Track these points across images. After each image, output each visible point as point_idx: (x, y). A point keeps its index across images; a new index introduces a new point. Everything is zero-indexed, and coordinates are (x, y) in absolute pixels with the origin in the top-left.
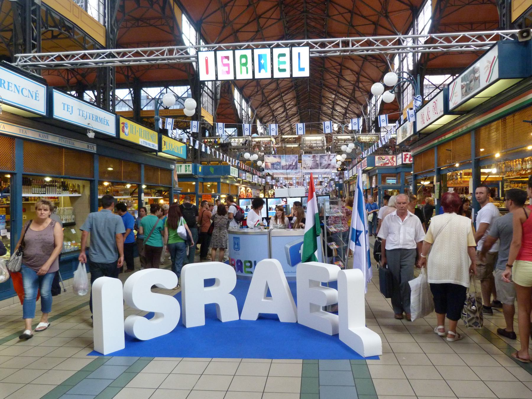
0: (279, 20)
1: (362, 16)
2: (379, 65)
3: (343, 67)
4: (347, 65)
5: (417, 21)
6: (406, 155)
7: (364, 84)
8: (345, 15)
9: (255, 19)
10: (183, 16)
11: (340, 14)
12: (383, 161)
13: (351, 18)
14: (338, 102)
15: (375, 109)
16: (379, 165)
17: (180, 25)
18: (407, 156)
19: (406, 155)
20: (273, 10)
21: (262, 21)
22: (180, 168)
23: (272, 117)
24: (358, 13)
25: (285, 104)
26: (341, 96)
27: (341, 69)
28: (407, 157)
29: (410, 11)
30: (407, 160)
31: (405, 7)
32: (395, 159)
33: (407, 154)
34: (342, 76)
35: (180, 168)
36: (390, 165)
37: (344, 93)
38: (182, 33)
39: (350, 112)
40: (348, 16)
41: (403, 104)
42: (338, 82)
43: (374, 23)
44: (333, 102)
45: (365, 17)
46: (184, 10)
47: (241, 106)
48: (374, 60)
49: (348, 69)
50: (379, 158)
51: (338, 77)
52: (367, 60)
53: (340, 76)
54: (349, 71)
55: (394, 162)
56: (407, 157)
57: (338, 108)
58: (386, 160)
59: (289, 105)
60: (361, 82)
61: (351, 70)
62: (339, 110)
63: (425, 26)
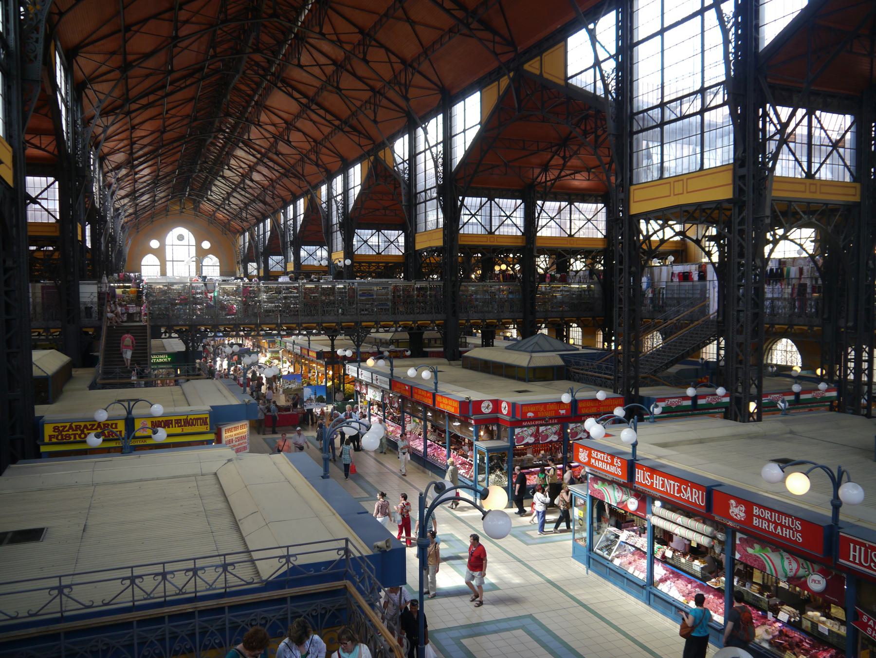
1: (354, 74)
2: (364, 141)
4: (298, 124)
5: (451, 113)
11: (318, 65)
24: (349, 67)
26: (271, 164)
37: (280, 161)
43: (372, 89)
45: (360, 79)
49: (299, 130)
54: (301, 134)
61: (305, 134)
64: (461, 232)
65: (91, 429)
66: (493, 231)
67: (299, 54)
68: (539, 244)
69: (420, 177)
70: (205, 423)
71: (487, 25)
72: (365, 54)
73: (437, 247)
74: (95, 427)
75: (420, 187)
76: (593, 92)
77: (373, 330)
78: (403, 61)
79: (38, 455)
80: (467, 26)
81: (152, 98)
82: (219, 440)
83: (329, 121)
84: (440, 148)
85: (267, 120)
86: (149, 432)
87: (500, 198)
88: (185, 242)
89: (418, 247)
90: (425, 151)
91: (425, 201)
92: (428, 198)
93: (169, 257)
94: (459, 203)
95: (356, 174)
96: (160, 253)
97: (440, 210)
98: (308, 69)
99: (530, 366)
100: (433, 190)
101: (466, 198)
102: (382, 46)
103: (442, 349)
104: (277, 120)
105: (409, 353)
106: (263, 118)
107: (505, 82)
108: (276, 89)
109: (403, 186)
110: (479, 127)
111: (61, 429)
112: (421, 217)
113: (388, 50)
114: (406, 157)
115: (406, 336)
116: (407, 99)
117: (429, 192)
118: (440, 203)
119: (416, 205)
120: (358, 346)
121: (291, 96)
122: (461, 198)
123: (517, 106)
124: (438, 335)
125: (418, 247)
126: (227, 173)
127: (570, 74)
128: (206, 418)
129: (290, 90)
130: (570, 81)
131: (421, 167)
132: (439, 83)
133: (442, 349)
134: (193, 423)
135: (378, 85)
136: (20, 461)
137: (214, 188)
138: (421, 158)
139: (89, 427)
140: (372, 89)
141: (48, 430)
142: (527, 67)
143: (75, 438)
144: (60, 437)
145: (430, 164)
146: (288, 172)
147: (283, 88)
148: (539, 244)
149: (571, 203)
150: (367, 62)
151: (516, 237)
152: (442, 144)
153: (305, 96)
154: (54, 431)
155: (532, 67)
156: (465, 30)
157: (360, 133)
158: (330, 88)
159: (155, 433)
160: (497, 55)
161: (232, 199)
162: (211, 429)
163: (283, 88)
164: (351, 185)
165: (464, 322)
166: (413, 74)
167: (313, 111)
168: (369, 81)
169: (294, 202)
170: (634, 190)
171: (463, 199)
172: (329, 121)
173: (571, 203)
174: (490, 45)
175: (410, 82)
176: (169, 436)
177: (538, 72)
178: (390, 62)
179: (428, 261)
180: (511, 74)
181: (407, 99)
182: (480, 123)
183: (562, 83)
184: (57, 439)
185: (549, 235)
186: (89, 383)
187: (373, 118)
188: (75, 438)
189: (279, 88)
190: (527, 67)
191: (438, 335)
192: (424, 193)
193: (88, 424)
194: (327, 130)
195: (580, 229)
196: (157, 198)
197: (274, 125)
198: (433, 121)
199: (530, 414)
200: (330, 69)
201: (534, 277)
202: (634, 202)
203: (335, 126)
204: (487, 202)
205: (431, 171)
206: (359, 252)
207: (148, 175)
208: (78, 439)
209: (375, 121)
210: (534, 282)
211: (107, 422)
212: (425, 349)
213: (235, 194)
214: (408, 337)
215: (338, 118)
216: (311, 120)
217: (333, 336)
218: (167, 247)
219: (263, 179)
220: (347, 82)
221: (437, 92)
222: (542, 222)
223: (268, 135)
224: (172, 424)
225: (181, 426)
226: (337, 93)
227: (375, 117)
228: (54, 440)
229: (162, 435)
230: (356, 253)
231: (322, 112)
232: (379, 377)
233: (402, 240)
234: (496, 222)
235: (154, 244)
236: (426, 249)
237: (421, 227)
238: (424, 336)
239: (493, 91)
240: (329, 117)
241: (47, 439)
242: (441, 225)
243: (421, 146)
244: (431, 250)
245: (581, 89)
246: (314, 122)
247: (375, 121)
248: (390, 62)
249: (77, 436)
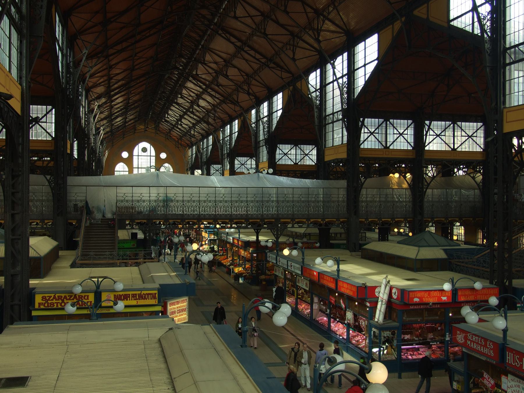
1: (277, 22)
2: (285, 75)
24: (273, 17)
26: (213, 93)
34: (228, 76)
43: (292, 34)
45: (282, 26)
48: (278, 68)
49: (235, 67)
51: (215, 72)
54: (236, 70)
64: (362, 147)
65: (70, 299)
66: (388, 146)
67: (236, 8)
68: (426, 156)
69: (329, 104)
70: (154, 298)
72: (286, 7)
73: (342, 159)
74: (72, 298)
75: (329, 111)
76: (471, 31)
77: (290, 225)
79: (31, 319)
82: (164, 312)
83: (258, 60)
84: (345, 79)
86: (111, 304)
87: (394, 119)
88: (148, 153)
89: (327, 159)
90: (333, 82)
91: (333, 122)
92: (335, 120)
93: (135, 165)
94: (360, 124)
95: (279, 100)
96: (129, 162)
97: (344, 129)
98: (243, 20)
99: (418, 258)
100: (339, 113)
101: (366, 119)
103: (345, 242)
104: (219, 60)
105: (318, 245)
106: (208, 58)
107: (398, 25)
108: (217, 35)
109: (316, 110)
110: (376, 62)
111: (47, 298)
112: (329, 136)
114: (318, 87)
115: (316, 231)
116: (319, 42)
117: (336, 114)
118: (345, 124)
120: (277, 238)
121: (228, 40)
122: (361, 119)
124: (342, 231)
125: (327, 159)
126: (180, 101)
127: (451, 18)
128: (156, 294)
129: (228, 35)
130: (452, 23)
131: (329, 96)
132: (345, 28)
133: (345, 242)
134: (145, 297)
135: (296, 30)
136: (15, 323)
138: (329, 88)
139: (68, 298)
140: (292, 34)
141: (38, 299)
142: (416, 13)
143: (57, 306)
144: (46, 305)
145: (337, 92)
146: (227, 99)
147: (223, 35)
148: (426, 156)
149: (454, 123)
150: (287, 13)
151: (407, 151)
152: (346, 77)
153: (239, 40)
154: (42, 300)
155: (420, 12)
157: (282, 68)
158: (258, 34)
159: (116, 304)
161: (183, 120)
162: (159, 302)
163: (223, 35)
164: (275, 109)
165: (363, 220)
166: (324, 22)
167: (246, 52)
168: (288, 28)
169: (231, 122)
170: (507, 112)
171: (364, 120)
172: (258, 60)
173: (454, 123)
175: (321, 28)
176: (126, 306)
177: (425, 17)
178: (306, 12)
179: (335, 170)
180: (403, 19)
181: (319, 42)
183: (446, 25)
184: (44, 306)
185: (435, 149)
186: (70, 263)
187: (292, 56)
188: (57, 306)
189: (220, 35)
190: (416, 13)
191: (342, 231)
192: (332, 116)
193: (67, 295)
194: (256, 66)
195: (462, 144)
196: (127, 120)
197: (216, 63)
198: (339, 59)
199: (416, 300)
200: (258, 19)
201: (423, 183)
202: (507, 122)
203: (263, 63)
204: (383, 122)
205: (338, 99)
206: (280, 162)
208: (59, 306)
209: (294, 60)
210: (422, 188)
211: (81, 294)
212: (331, 242)
213: (186, 117)
214: (318, 232)
215: (264, 57)
216: (244, 59)
217: (257, 230)
218: (134, 157)
219: (207, 104)
220: (271, 28)
222: (429, 139)
223: (211, 71)
224: (129, 297)
225: (136, 299)
226: (264, 38)
227: (294, 56)
228: (42, 307)
229: (120, 306)
230: (278, 163)
231: (252, 53)
232: (293, 264)
233: (314, 152)
234: (390, 139)
235: (125, 155)
236: (333, 161)
237: (329, 144)
238: (331, 231)
239: (388, 32)
240: (258, 56)
241: (37, 306)
242: (345, 141)
243: (330, 78)
244: (337, 161)
245: (462, 29)
246: (247, 60)
247: (294, 60)
248: (306, 12)
249: (59, 304)
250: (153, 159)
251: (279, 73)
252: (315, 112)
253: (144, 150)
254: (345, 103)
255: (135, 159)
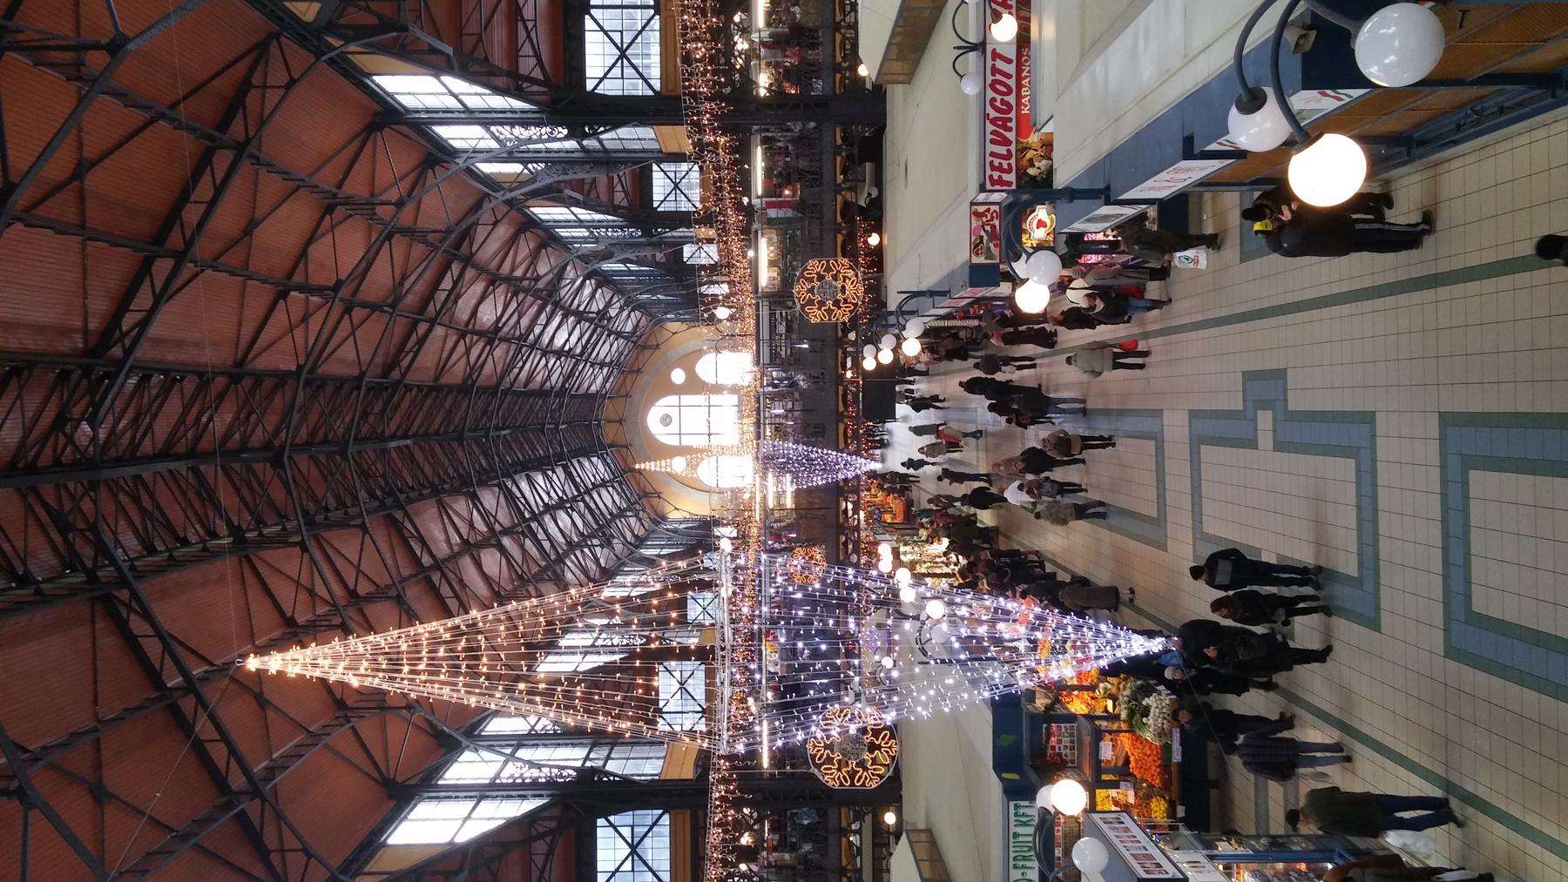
0: (364, 528)
3: (471, 326)
4: (465, 317)
5: (418, 112)
6: (993, 182)
7: (519, 259)
8: (356, 321)
9: (361, 611)
10: (391, 841)
12: (985, 241)
13: (364, 305)
14: (547, 341)
15: (607, 228)
16: (995, 251)
17: (433, 853)
18: (996, 177)
19: (993, 182)
20: (328, 548)
21: (363, 588)
22: (1021, 839)
23: (586, 550)
25: (546, 505)
27: (474, 332)
28: (1000, 177)
29: (387, 131)
30: (1006, 177)
31: (368, 149)
32: (981, 209)
33: (991, 176)
35: (1021, 839)
36: (996, 222)
38: (451, 843)
39: (576, 302)
40: (358, 313)
41: (644, 151)
42: (505, 339)
43: (389, 237)
44: (545, 353)
46: (372, 842)
47: (586, 651)
50: (977, 254)
52: (472, 255)
53: (492, 336)
55: (988, 210)
56: (1000, 177)
57: (559, 342)
58: (983, 233)
59: (548, 494)
60: (513, 270)
62: (566, 336)
63: (452, 94)
71: (235, 104)
78: (329, 209)
80: (240, 148)
81: (445, 590)
85: (461, 367)
88: (673, 413)
93: (699, 442)
95: (546, 212)
102: (303, 254)
104: (461, 348)
106: (457, 372)
110: (443, 78)
113: (309, 242)
119: (605, 150)
123: (394, 34)
129: (404, 354)
137: (586, 385)
147: (405, 363)
156: (251, 149)
160: (292, 83)
163: (405, 363)
174: (272, 97)
182: (437, 76)
197: (468, 351)
207: (571, 517)
216: (456, 302)
219: (564, 327)
221: (379, 138)
247: (448, 231)
248: (332, 229)
250: (687, 399)
251: (481, 232)
252: (575, 177)
253: (666, 420)
254: (552, 133)
255: (686, 441)
